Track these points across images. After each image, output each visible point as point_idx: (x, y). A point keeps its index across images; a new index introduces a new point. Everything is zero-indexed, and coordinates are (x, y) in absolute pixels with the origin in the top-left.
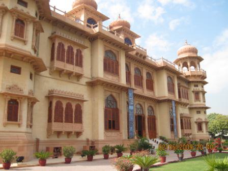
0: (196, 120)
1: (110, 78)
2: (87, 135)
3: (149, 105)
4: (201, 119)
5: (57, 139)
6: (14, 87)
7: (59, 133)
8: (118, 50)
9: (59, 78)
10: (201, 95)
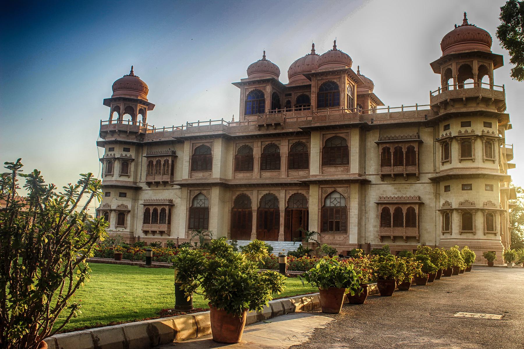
0: (444, 205)
1: (199, 177)
2: (173, 236)
3: (292, 193)
5: (153, 237)
6: (107, 205)
7: (154, 233)
8: (211, 141)
10: (455, 150)
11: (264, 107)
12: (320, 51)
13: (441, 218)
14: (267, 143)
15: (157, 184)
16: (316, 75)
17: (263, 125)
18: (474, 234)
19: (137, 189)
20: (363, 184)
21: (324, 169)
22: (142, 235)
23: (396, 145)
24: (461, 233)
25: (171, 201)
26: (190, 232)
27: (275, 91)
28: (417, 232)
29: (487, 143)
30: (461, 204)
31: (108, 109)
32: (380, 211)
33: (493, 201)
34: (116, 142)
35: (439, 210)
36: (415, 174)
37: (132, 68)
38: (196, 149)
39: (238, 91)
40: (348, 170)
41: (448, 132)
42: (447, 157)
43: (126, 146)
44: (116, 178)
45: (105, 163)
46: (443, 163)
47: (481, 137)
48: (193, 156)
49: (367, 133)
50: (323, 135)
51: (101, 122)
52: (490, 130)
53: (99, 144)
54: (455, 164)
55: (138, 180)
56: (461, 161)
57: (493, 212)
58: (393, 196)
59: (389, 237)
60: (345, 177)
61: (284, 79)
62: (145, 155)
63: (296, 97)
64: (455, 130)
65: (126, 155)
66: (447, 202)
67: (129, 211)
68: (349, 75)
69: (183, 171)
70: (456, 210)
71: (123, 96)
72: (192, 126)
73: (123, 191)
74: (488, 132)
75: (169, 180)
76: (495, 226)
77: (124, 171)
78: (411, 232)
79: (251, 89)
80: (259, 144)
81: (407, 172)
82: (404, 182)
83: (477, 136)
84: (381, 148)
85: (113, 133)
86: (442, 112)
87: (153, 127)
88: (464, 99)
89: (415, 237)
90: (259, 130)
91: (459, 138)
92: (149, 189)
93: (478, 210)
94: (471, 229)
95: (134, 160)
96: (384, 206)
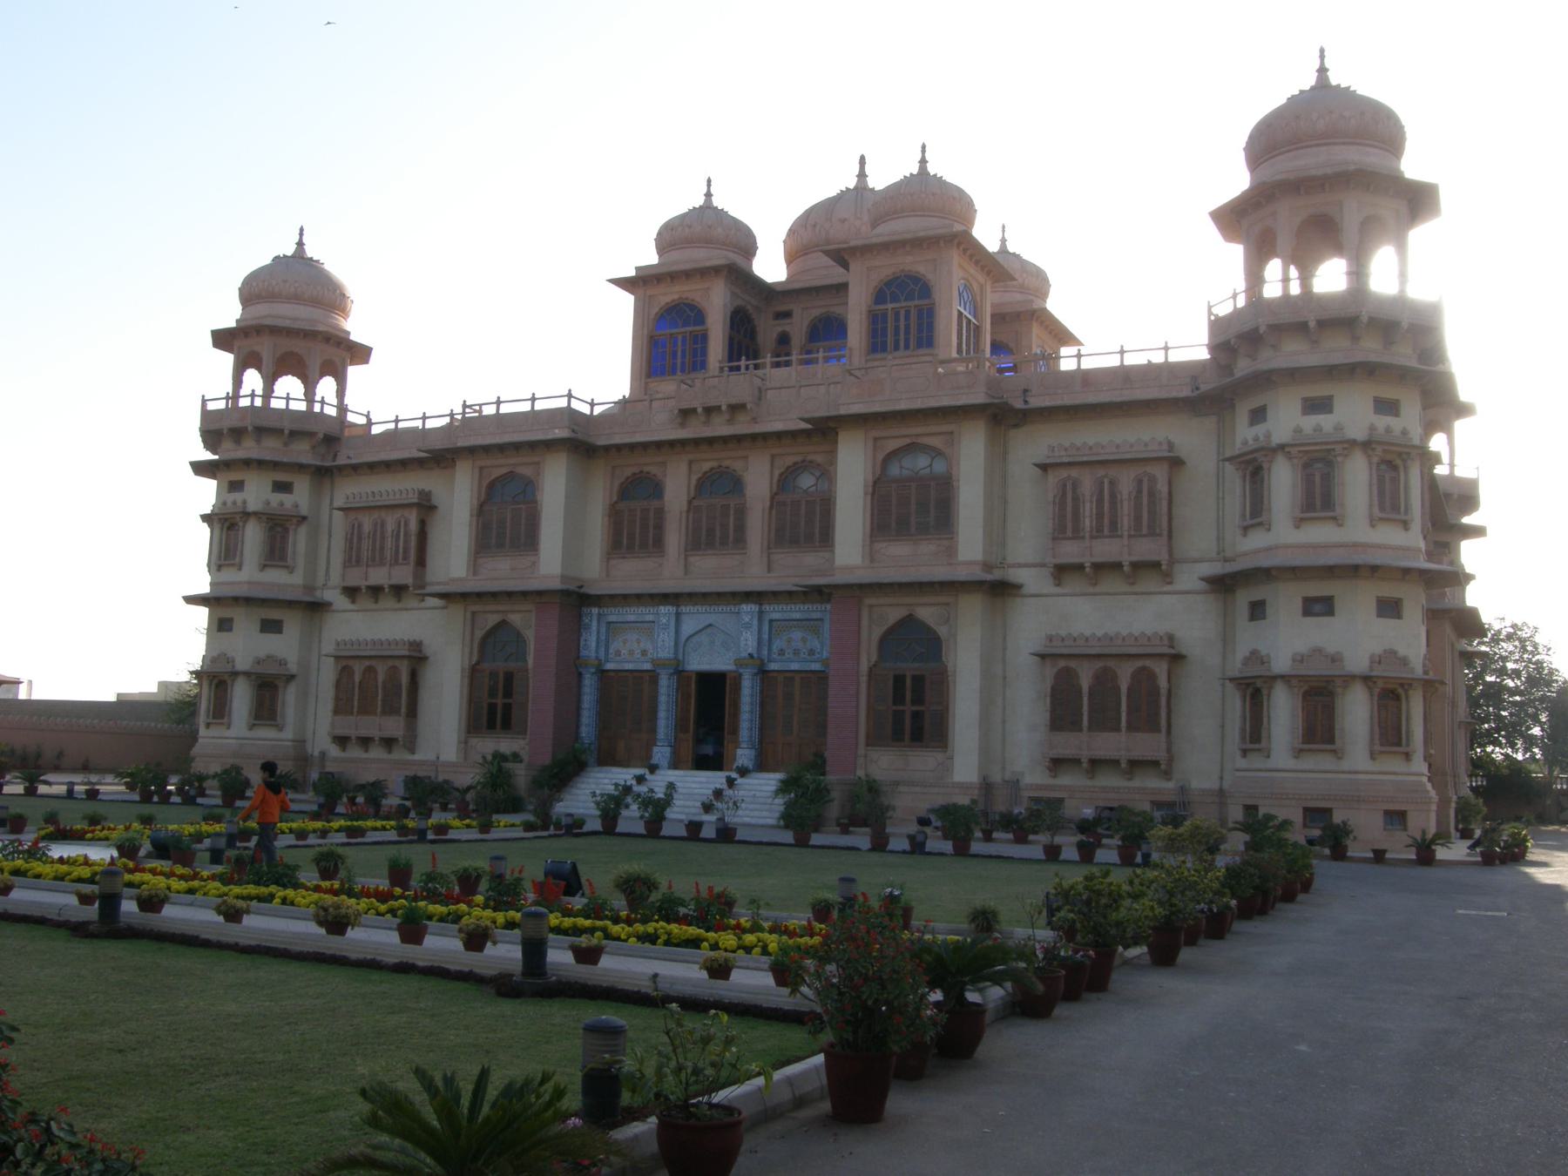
1: (502, 572)
4: (1404, 662)
5: (365, 755)
7: (365, 742)
8: (536, 459)
9: (374, 606)
11: (704, 352)
12: (879, 180)
13: (1238, 703)
14: (706, 466)
15: (376, 591)
16: (866, 250)
17: (694, 410)
18: (1337, 754)
19: (316, 608)
20: (999, 589)
21: (878, 546)
22: (334, 751)
23: (1101, 472)
24: (1298, 753)
25: (416, 645)
26: (474, 741)
27: (739, 302)
28: (1164, 746)
29: (1383, 467)
30: (1299, 659)
31: (227, 360)
32: (1049, 682)
33: (1402, 652)
34: (247, 463)
35: (1231, 680)
36: (1155, 565)
37: (301, 234)
38: (491, 486)
39: (627, 301)
40: (951, 551)
41: (1260, 429)
42: (1256, 512)
43: (282, 474)
44: (249, 575)
45: (217, 527)
46: (1246, 529)
47: (1367, 445)
48: (481, 506)
49: (1013, 433)
50: (876, 439)
51: (204, 401)
52: (1395, 423)
53: (200, 468)
54: (1286, 535)
55: (320, 580)
56: (1299, 523)
57: (1402, 685)
58: (1088, 633)
59: (1075, 762)
60: (940, 573)
61: (770, 266)
62: (339, 502)
63: (806, 323)
64: (1286, 419)
65: (282, 504)
66: (1254, 653)
67: (292, 677)
68: (965, 251)
69: (453, 556)
70: (1285, 678)
71: (268, 322)
72: (480, 411)
73: (274, 614)
74: (1388, 430)
75: (409, 580)
76: (1408, 732)
77: (275, 553)
78: (1145, 745)
79: (669, 295)
80: (684, 468)
81: (1134, 559)
82: (1127, 588)
83: (1353, 443)
84: (1053, 478)
85: (237, 434)
86: (1243, 367)
87: (368, 416)
88: (1312, 324)
89: (1156, 764)
90: (683, 425)
91: (1294, 450)
92: (352, 607)
93: (1350, 679)
94: (1331, 740)
95: (304, 518)
96: (1062, 663)
